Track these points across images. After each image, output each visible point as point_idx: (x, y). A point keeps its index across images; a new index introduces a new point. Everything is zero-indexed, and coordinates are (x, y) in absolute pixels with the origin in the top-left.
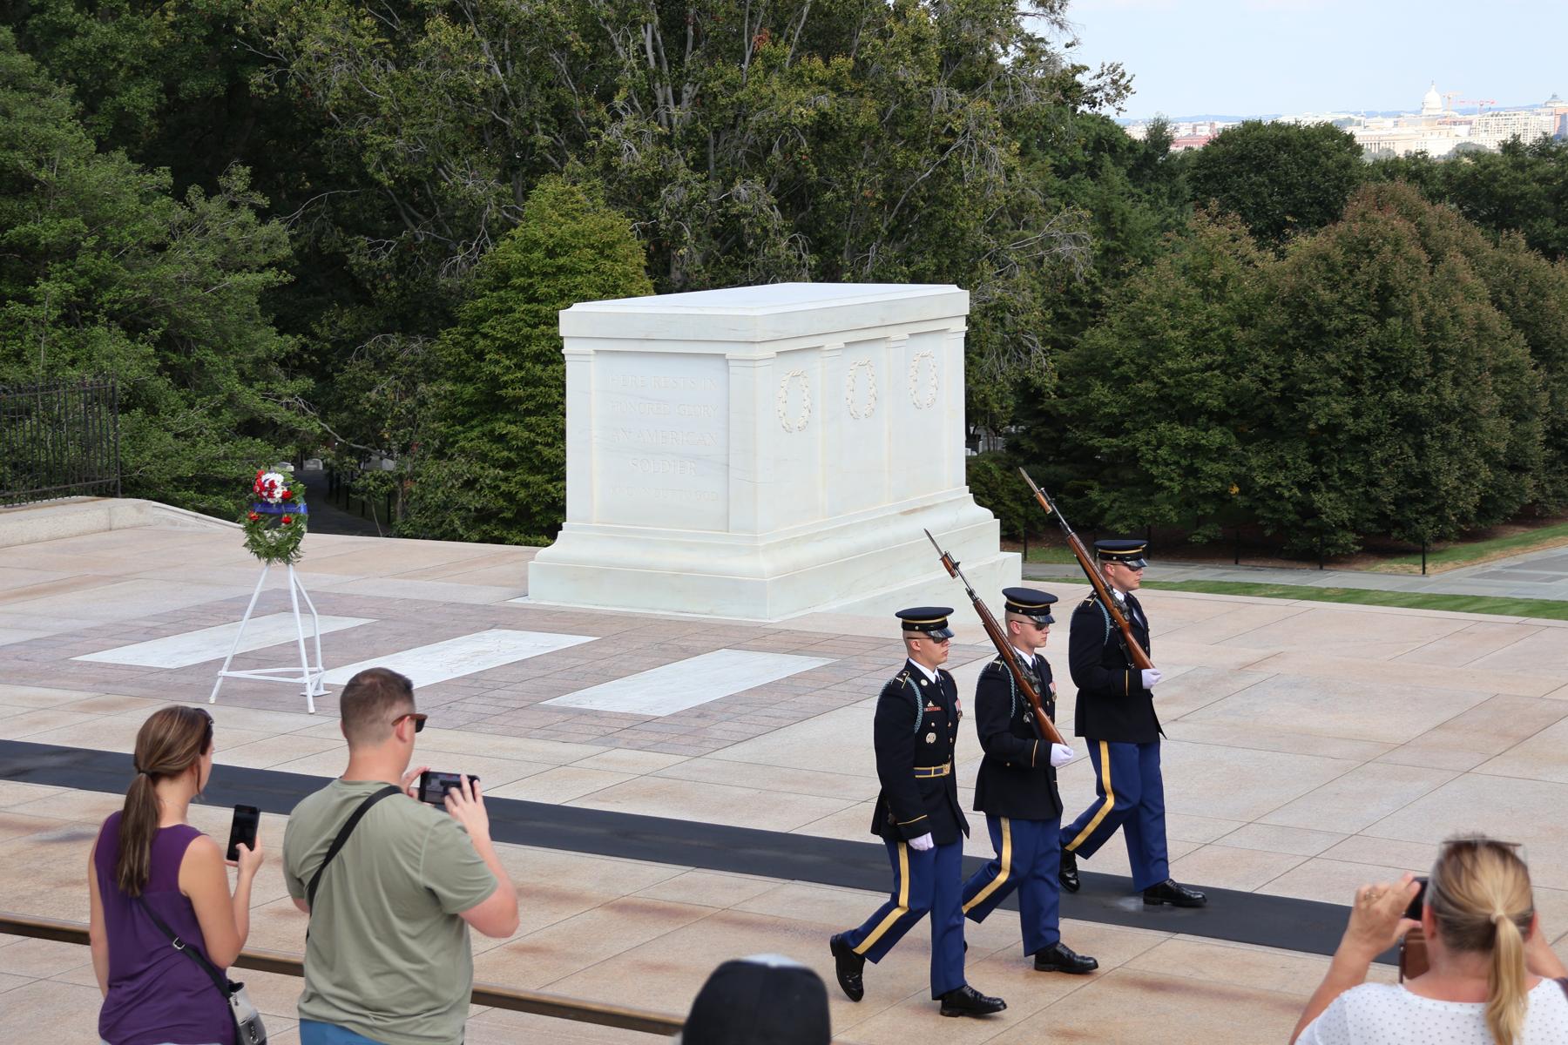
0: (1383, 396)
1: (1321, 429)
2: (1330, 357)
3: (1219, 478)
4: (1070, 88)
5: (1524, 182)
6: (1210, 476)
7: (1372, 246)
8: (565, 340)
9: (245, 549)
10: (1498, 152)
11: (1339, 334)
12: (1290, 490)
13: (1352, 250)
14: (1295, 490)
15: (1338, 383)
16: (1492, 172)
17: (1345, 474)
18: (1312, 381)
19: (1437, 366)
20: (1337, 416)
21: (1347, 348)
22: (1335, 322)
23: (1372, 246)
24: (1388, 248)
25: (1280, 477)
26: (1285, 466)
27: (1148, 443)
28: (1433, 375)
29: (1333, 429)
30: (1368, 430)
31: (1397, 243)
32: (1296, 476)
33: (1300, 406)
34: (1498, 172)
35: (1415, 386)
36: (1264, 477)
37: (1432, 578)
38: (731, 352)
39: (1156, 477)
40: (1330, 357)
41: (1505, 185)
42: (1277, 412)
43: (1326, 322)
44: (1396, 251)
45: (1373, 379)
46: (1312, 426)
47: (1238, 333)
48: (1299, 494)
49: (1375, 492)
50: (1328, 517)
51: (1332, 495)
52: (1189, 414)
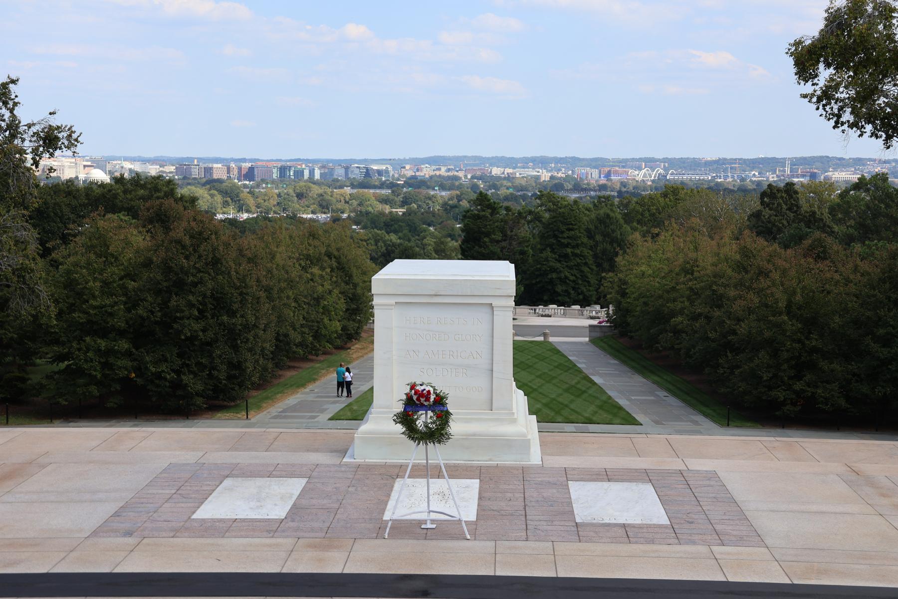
0: (218, 320)
1: (187, 339)
2: (191, 298)
3: (126, 369)
4: (54, 139)
5: (131, 200)
6: (120, 368)
7: (205, 235)
8: (375, 298)
9: (403, 436)
10: (113, 183)
11: (195, 284)
12: (169, 374)
13: (192, 237)
14: (173, 374)
15: (196, 313)
16: (114, 194)
17: (198, 364)
18: (183, 311)
19: (243, 302)
20: (195, 331)
21: (199, 292)
22: (191, 278)
23: (205, 235)
24: (213, 236)
25: (163, 367)
26: (166, 360)
27: (79, 350)
28: (242, 307)
29: (192, 339)
30: (211, 338)
31: (216, 234)
32: (171, 366)
33: (175, 326)
34: (118, 194)
35: (232, 314)
36: (153, 367)
37: (253, 420)
38: (495, 302)
39: (87, 369)
40: (191, 298)
41: (121, 201)
42: (158, 329)
43: (186, 278)
44: (217, 239)
45: (211, 309)
46: (183, 337)
47: (131, 285)
48: (175, 377)
49: (215, 373)
50: (191, 389)
51: (192, 376)
52: (104, 333)
